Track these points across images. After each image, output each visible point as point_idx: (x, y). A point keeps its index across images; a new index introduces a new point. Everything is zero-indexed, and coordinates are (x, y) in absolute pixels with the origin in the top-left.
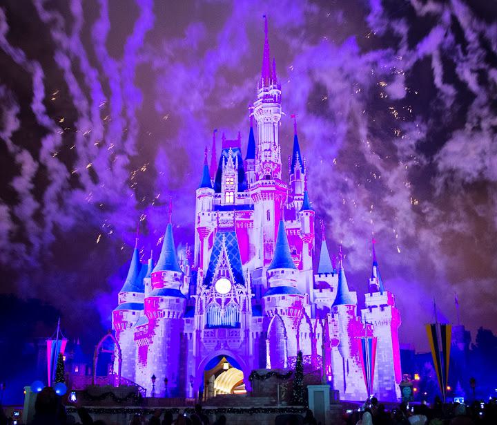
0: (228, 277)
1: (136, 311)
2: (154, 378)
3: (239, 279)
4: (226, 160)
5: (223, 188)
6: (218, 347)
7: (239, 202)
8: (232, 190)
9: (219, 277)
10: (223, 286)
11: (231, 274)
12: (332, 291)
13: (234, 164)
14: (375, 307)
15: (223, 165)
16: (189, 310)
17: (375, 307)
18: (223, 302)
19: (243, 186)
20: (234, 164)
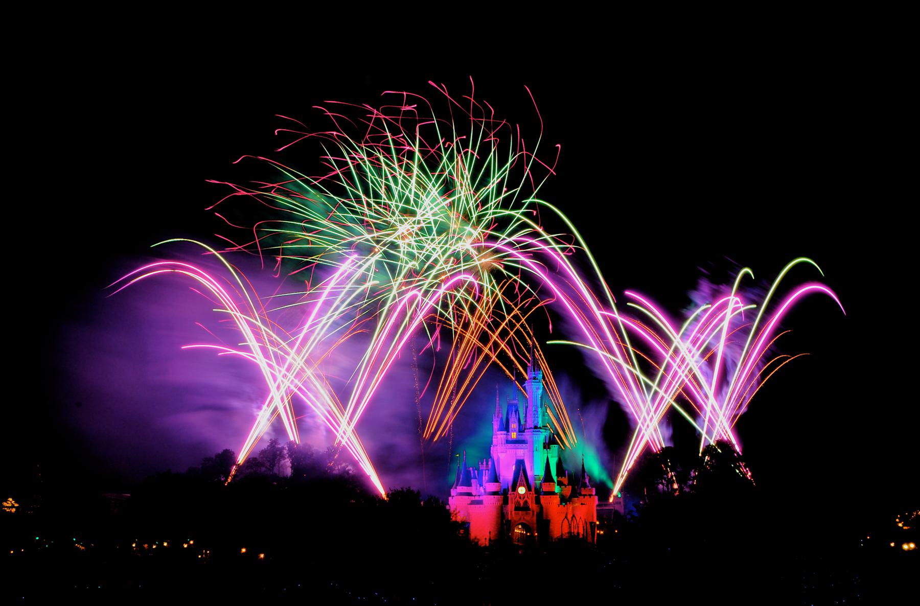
0: (524, 486)
1: (469, 497)
2: (490, 532)
3: (529, 488)
4: (511, 414)
5: (510, 430)
6: (521, 518)
7: (521, 438)
8: (515, 431)
9: (520, 486)
10: (522, 490)
11: (525, 485)
12: (566, 487)
13: (516, 416)
14: (586, 495)
15: (510, 416)
16: (506, 501)
17: (586, 495)
18: (522, 497)
19: (521, 430)
20: (516, 416)
